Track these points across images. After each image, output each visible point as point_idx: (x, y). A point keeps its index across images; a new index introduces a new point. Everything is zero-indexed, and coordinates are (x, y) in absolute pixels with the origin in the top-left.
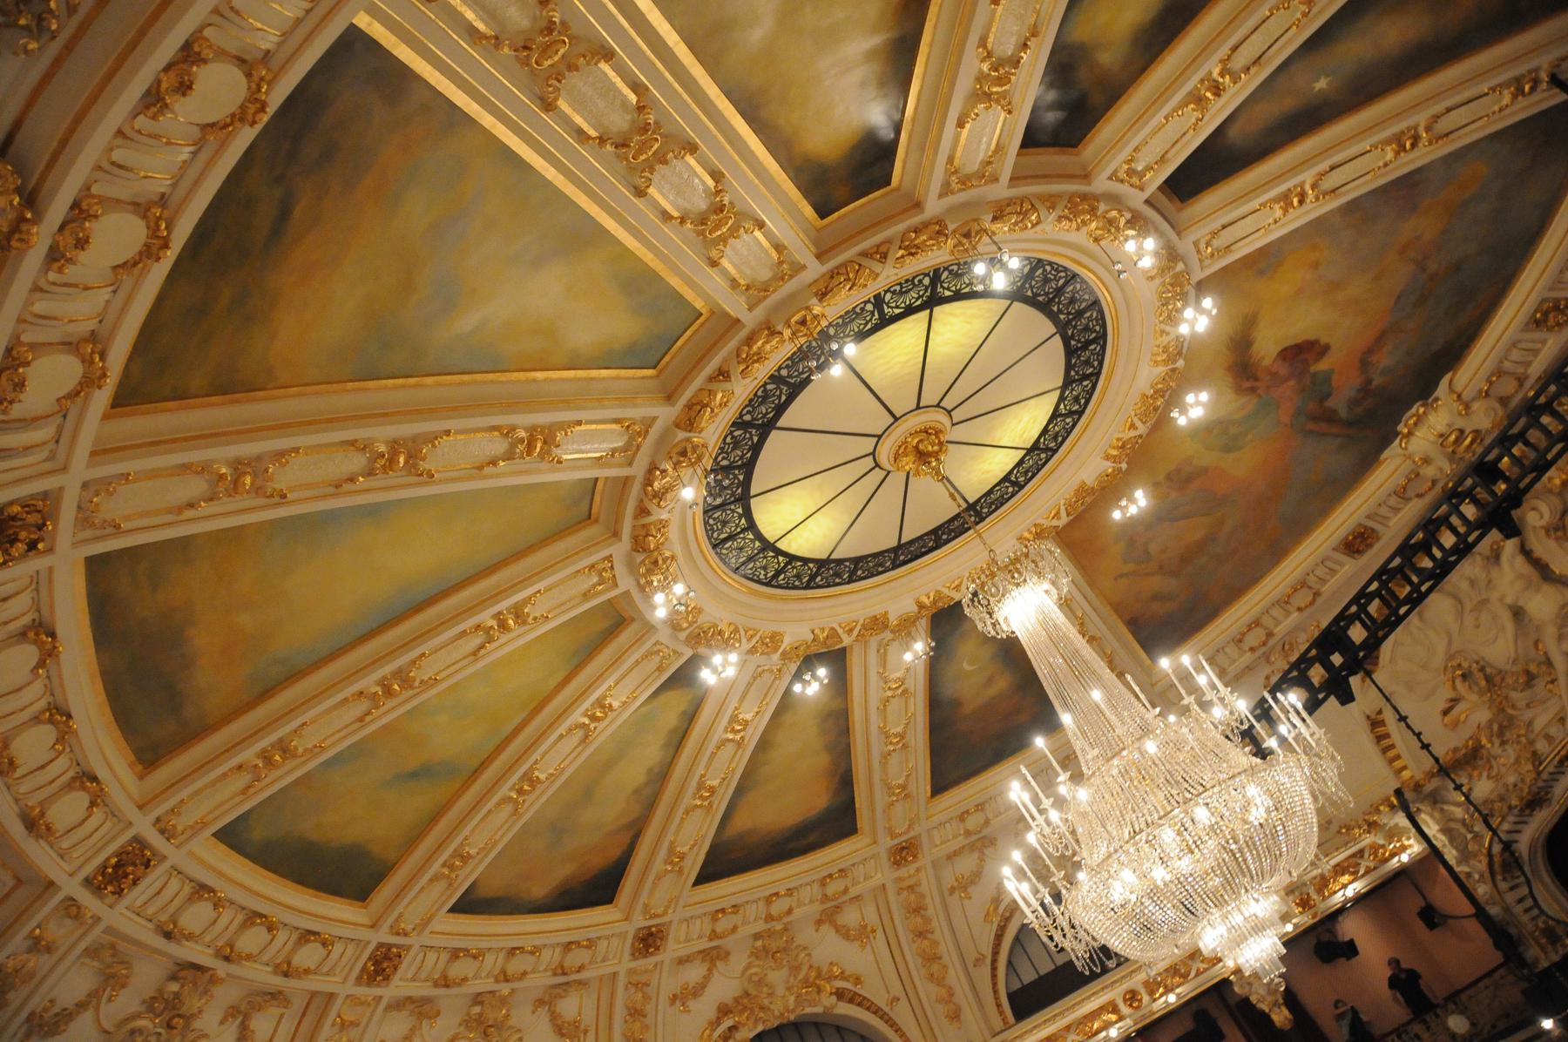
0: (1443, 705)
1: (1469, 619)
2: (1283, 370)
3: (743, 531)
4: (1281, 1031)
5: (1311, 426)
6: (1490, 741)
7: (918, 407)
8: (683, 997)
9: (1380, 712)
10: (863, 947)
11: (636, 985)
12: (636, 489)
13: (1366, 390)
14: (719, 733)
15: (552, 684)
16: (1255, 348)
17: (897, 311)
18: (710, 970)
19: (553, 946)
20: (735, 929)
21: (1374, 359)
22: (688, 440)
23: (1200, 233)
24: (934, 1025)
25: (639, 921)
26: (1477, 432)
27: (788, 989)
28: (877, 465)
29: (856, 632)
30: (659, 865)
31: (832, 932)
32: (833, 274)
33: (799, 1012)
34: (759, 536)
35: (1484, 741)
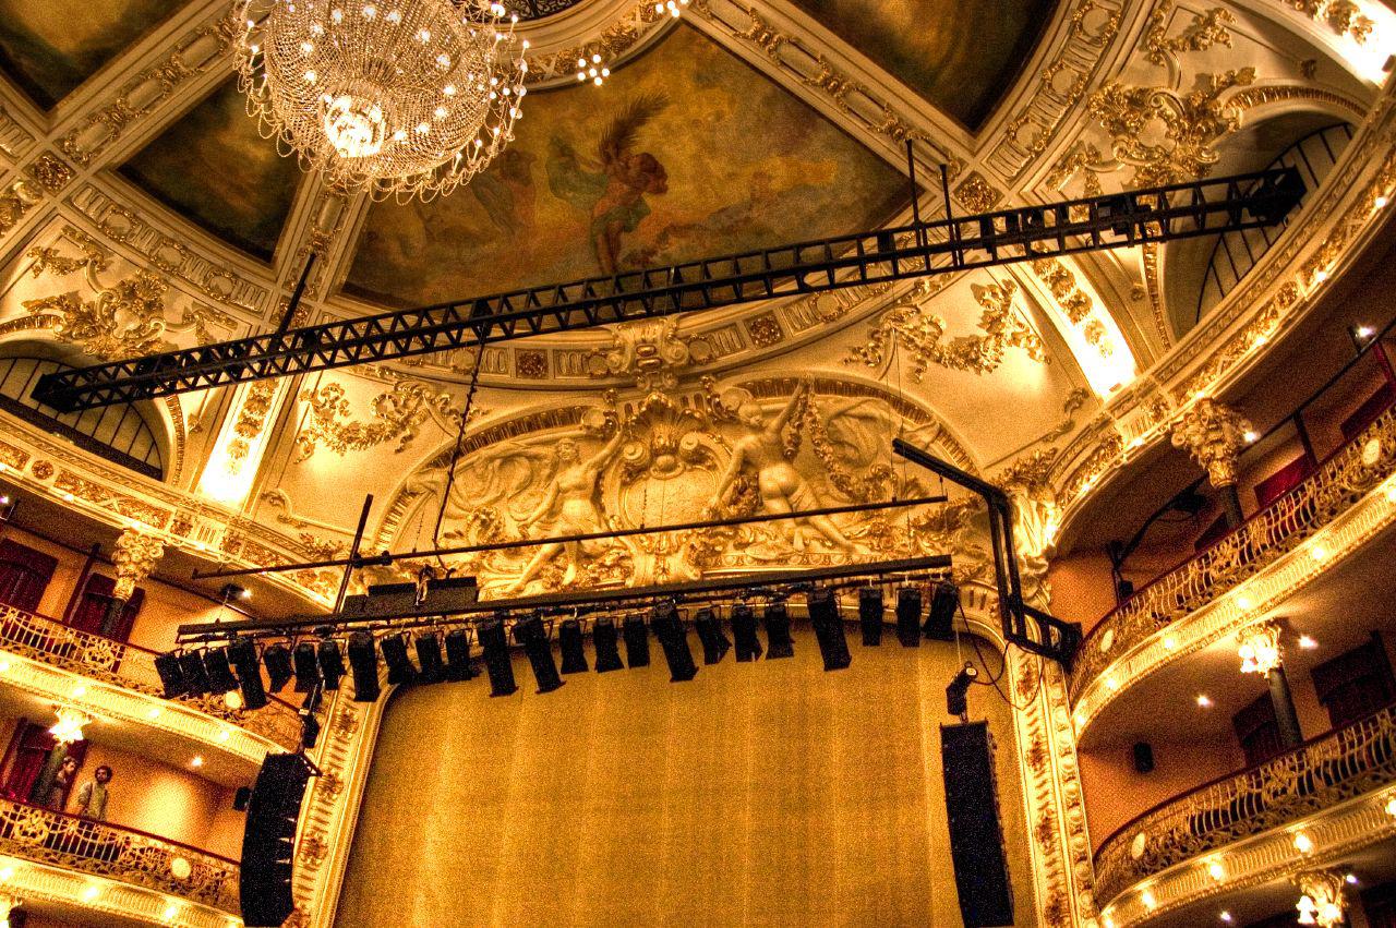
5: (600, 238)
9: (413, 494)
16: (641, 129)
21: (672, 239)
26: (662, 361)
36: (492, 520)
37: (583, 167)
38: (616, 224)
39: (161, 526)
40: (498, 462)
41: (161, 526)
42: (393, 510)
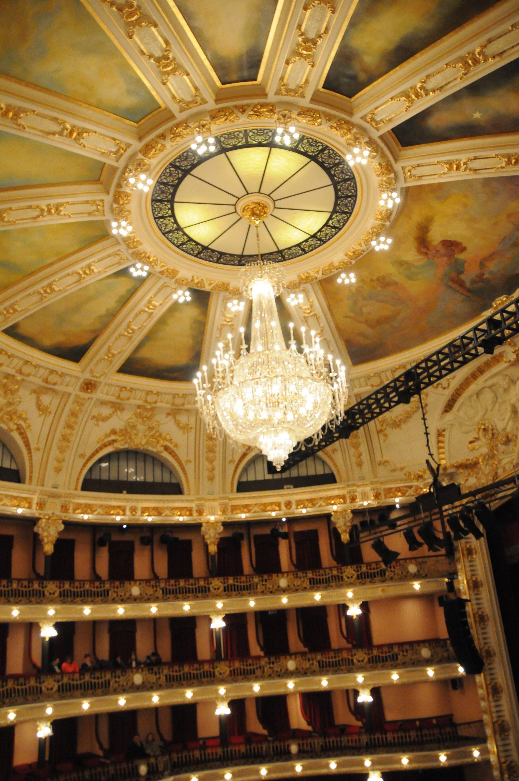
0: (471, 439)
1: (497, 406)
2: (442, 251)
3: (169, 216)
4: (342, 543)
5: (450, 284)
6: (483, 462)
7: (269, 195)
8: (99, 419)
9: (444, 430)
10: (184, 433)
11: (78, 403)
12: (118, 173)
13: (480, 278)
14: (142, 305)
15: (71, 250)
17: (254, 142)
18: (113, 412)
19: (46, 369)
20: (128, 399)
21: (487, 264)
22: (142, 160)
23: (408, 163)
24: (201, 479)
25: (87, 376)
27: (145, 436)
28: (236, 212)
29: (212, 286)
30: (102, 354)
31: (172, 421)
32: (220, 110)
33: (146, 447)
34: (176, 222)
35: (480, 461)
36: (488, 427)
37: (416, 264)
38: (454, 274)
39: (345, 502)
40: (475, 397)
41: (345, 502)
42: (439, 442)
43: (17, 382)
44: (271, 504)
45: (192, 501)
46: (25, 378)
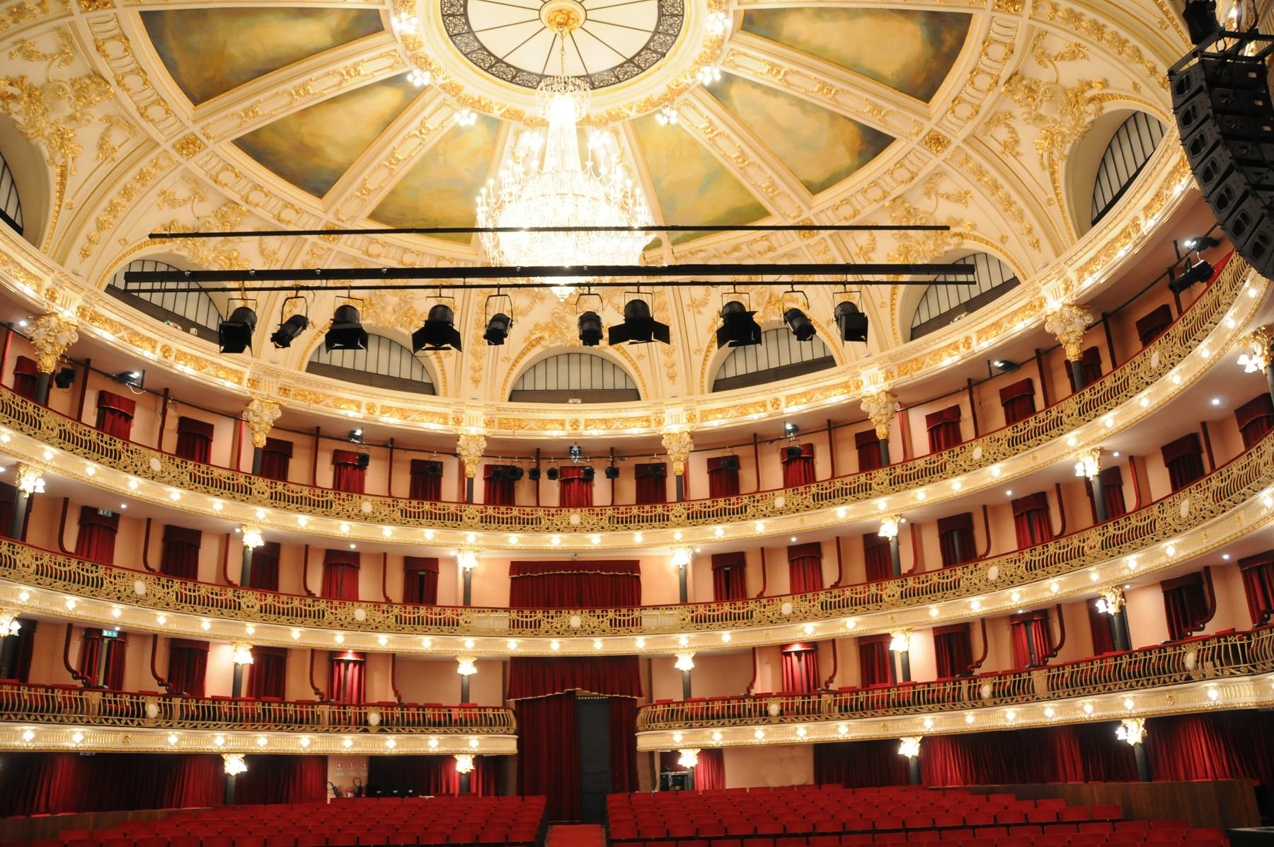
30: (353, 189)
34: (467, 23)
43: (242, 214)
44: (552, 421)
45: (448, 405)
46: (252, 209)
